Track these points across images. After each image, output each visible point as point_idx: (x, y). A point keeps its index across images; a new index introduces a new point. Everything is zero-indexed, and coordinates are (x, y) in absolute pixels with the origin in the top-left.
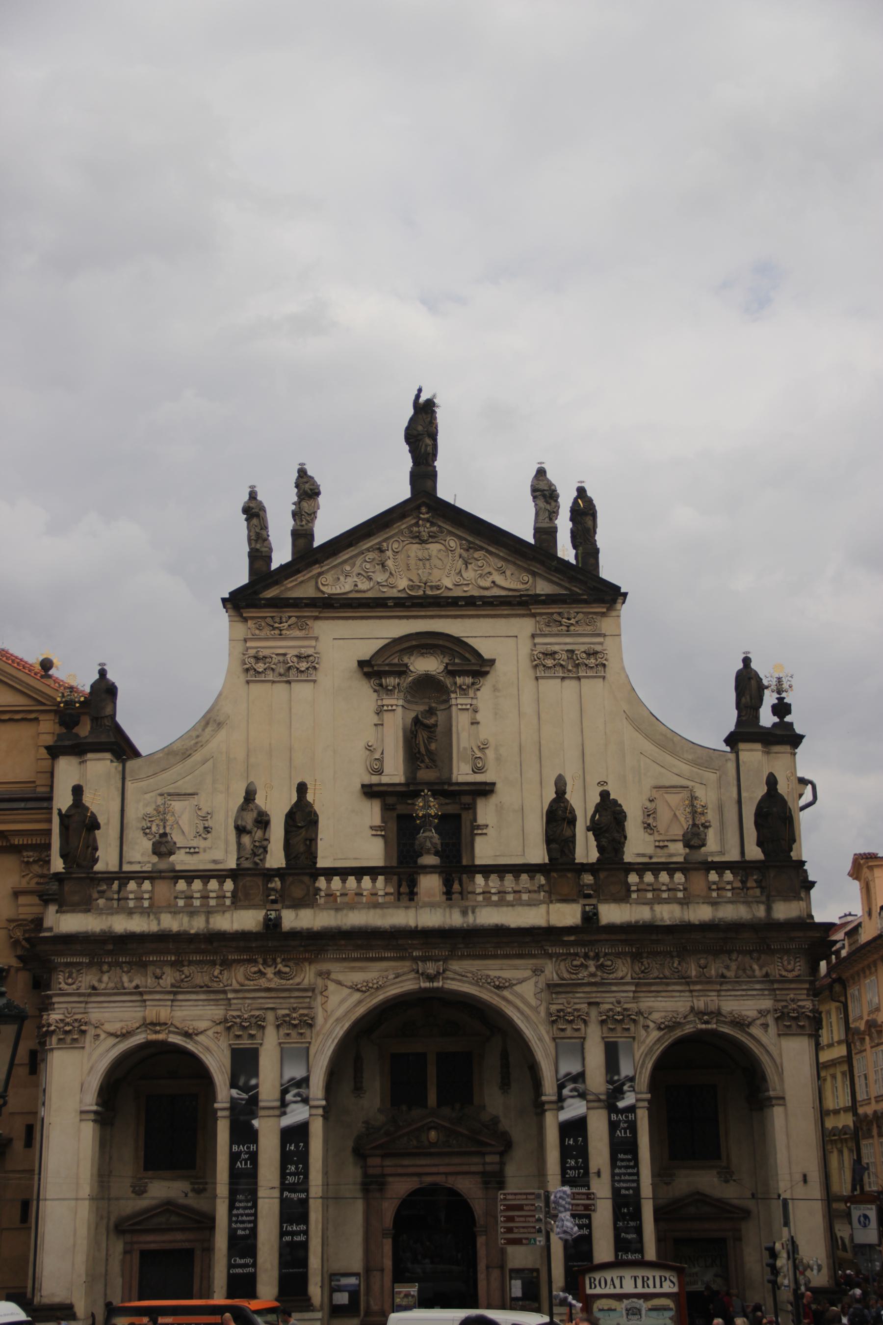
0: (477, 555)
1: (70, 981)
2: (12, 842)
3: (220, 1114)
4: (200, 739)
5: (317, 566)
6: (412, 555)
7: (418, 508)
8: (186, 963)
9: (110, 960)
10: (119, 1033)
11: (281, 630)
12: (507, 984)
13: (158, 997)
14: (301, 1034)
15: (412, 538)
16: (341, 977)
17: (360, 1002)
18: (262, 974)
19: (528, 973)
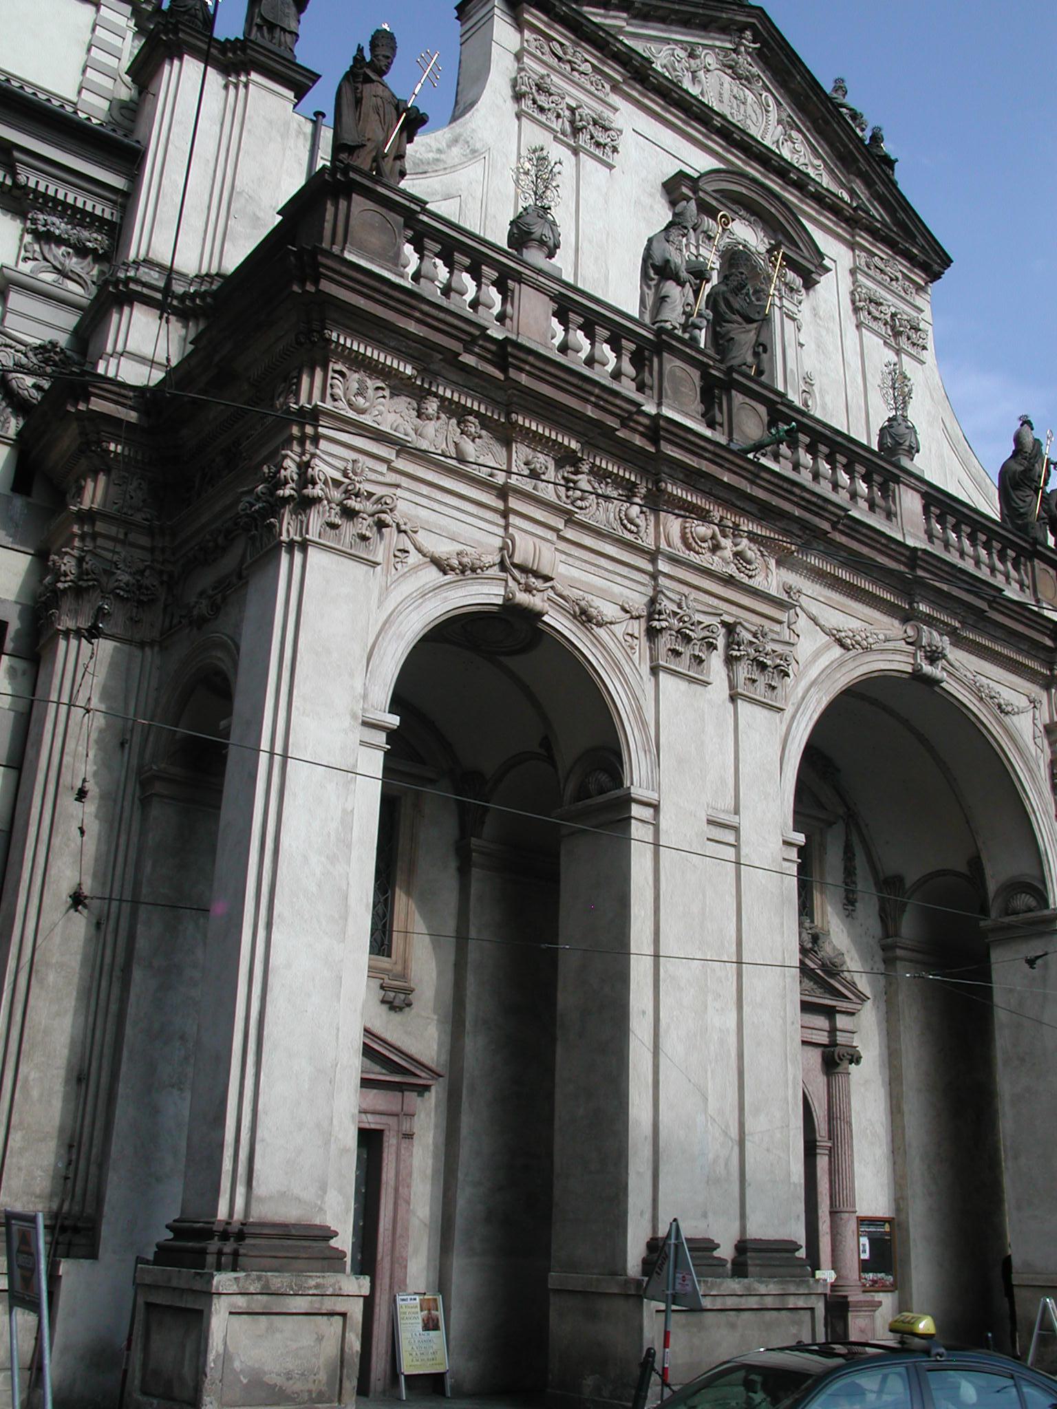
0: (794, 134)
1: (361, 400)
2: (22, 179)
3: (636, 810)
4: (443, 156)
5: (625, 15)
6: (726, 86)
7: (742, 28)
8: (585, 468)
9: (448, 394)
10: (455, 562)
11: (573, 69)
12: (1009, 708)
13: (539, 514)
14: (774, 688)
15: (725, 66)
16: (814, 608)
17: (842, 663)
18: (716, 548)
19: (1023, 702)
